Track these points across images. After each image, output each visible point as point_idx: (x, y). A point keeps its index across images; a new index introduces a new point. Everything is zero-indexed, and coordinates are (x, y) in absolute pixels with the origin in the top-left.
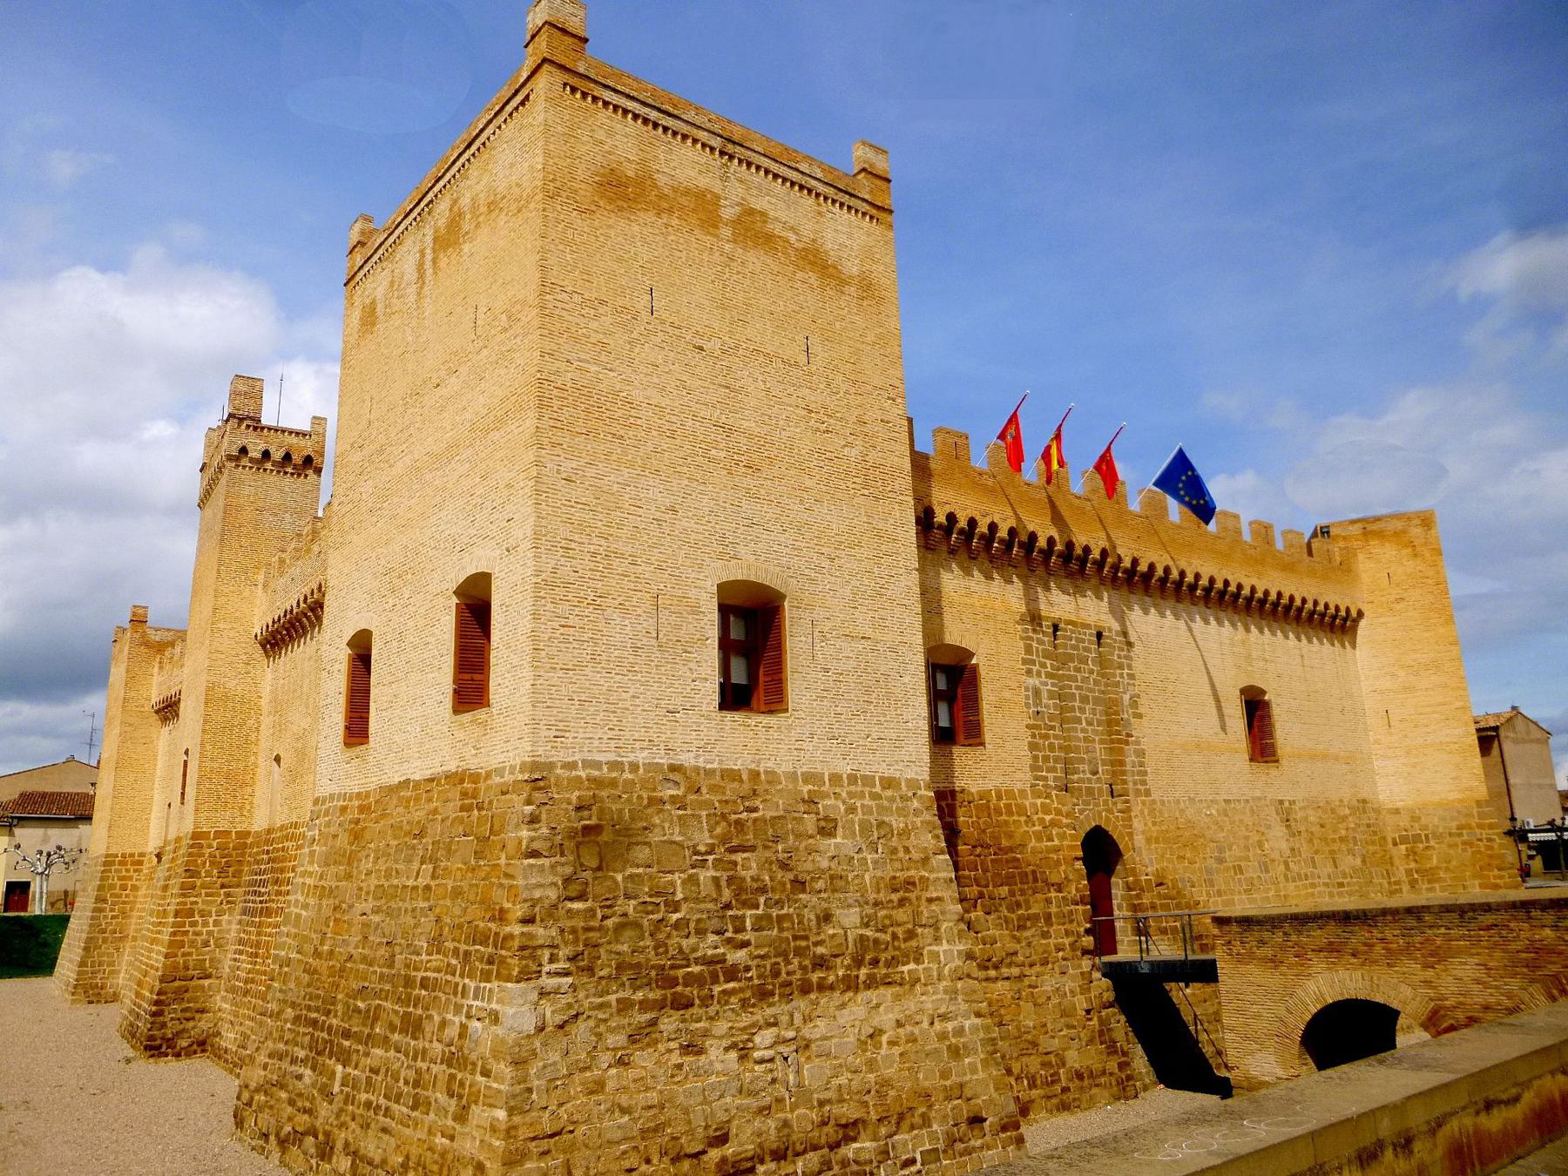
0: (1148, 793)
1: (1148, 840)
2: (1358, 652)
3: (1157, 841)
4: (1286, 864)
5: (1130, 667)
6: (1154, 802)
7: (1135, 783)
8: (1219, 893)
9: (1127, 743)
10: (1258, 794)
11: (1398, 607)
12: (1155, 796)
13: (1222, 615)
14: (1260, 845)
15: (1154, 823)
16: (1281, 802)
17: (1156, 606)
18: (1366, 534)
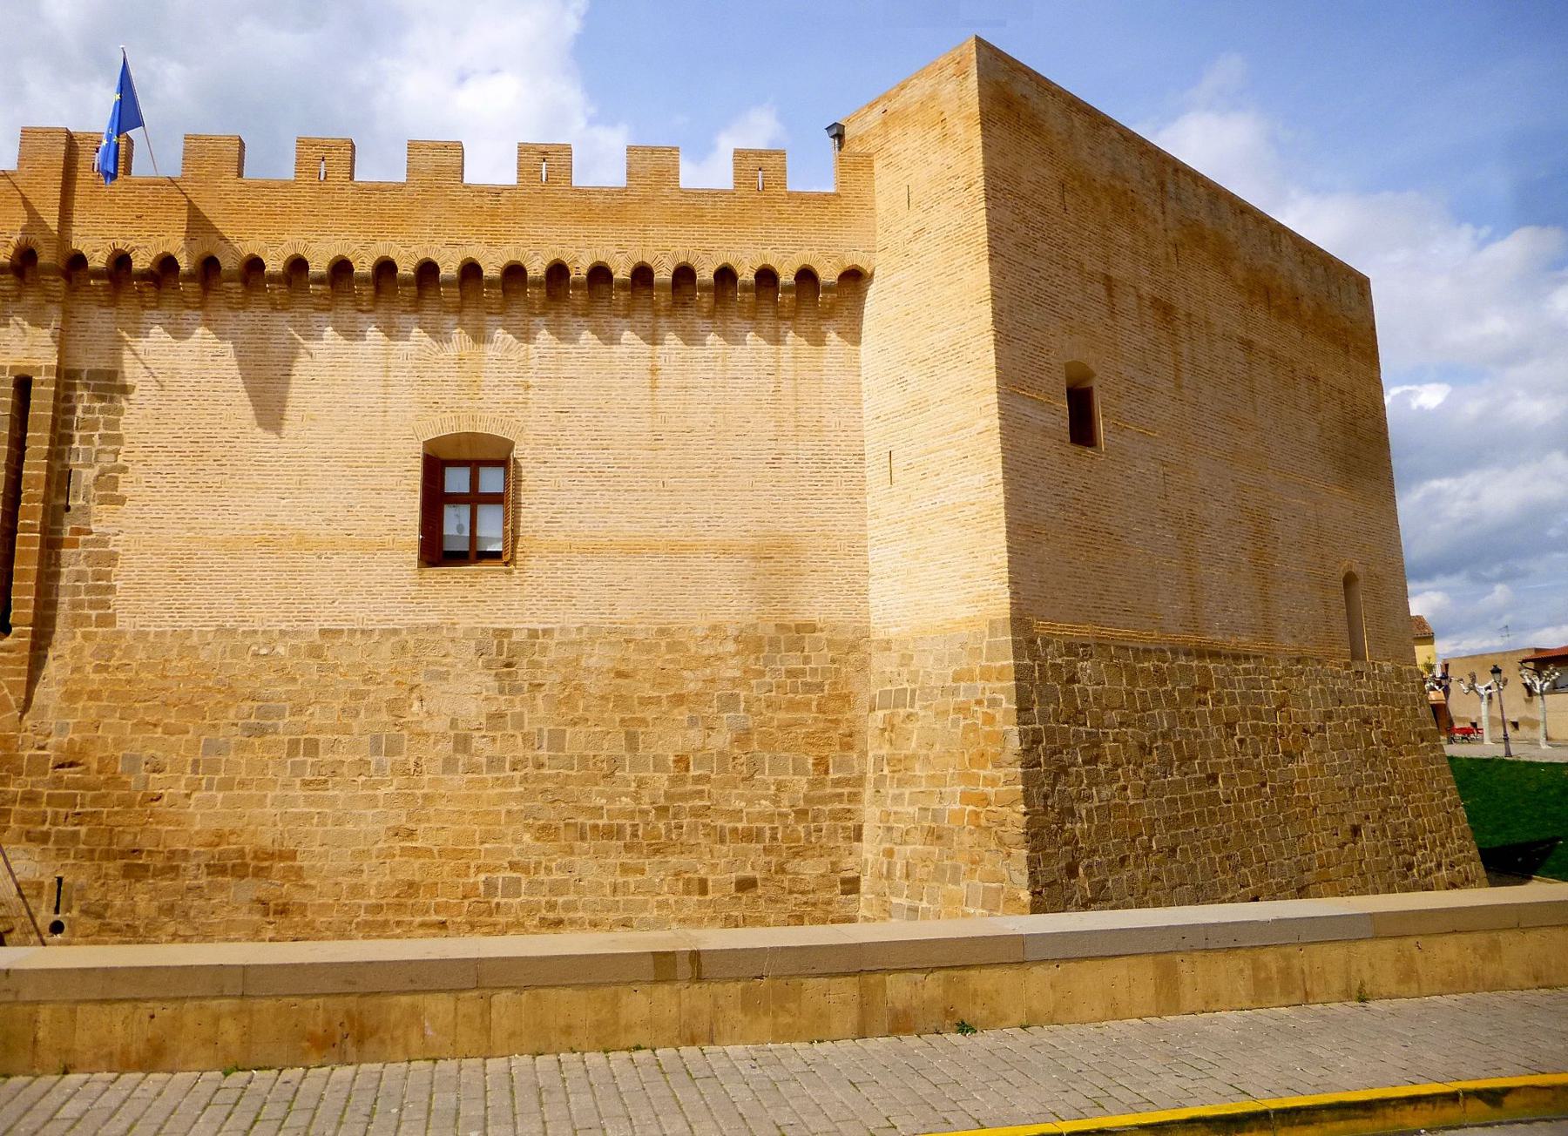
0: (106, 620)
1: (71, 696)
2: (862, 348)
3: (94, 695)
4: (463, 743)
5: (112, 425)
6: (120, 635)
7: (76, 605)
8: (226, 785)
9: (74, 544)
10: (432, 618)
11: (915, 247)
12: (124, 623)
13: (402, 320)
14: (395, 707)
15: (99, 669)
16: (507, 633)
17: (207, 323)
18: (888, 119)
